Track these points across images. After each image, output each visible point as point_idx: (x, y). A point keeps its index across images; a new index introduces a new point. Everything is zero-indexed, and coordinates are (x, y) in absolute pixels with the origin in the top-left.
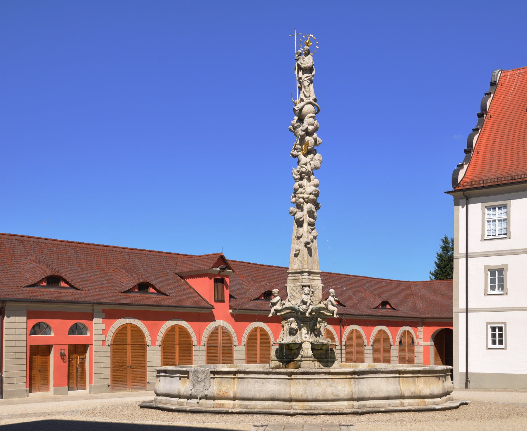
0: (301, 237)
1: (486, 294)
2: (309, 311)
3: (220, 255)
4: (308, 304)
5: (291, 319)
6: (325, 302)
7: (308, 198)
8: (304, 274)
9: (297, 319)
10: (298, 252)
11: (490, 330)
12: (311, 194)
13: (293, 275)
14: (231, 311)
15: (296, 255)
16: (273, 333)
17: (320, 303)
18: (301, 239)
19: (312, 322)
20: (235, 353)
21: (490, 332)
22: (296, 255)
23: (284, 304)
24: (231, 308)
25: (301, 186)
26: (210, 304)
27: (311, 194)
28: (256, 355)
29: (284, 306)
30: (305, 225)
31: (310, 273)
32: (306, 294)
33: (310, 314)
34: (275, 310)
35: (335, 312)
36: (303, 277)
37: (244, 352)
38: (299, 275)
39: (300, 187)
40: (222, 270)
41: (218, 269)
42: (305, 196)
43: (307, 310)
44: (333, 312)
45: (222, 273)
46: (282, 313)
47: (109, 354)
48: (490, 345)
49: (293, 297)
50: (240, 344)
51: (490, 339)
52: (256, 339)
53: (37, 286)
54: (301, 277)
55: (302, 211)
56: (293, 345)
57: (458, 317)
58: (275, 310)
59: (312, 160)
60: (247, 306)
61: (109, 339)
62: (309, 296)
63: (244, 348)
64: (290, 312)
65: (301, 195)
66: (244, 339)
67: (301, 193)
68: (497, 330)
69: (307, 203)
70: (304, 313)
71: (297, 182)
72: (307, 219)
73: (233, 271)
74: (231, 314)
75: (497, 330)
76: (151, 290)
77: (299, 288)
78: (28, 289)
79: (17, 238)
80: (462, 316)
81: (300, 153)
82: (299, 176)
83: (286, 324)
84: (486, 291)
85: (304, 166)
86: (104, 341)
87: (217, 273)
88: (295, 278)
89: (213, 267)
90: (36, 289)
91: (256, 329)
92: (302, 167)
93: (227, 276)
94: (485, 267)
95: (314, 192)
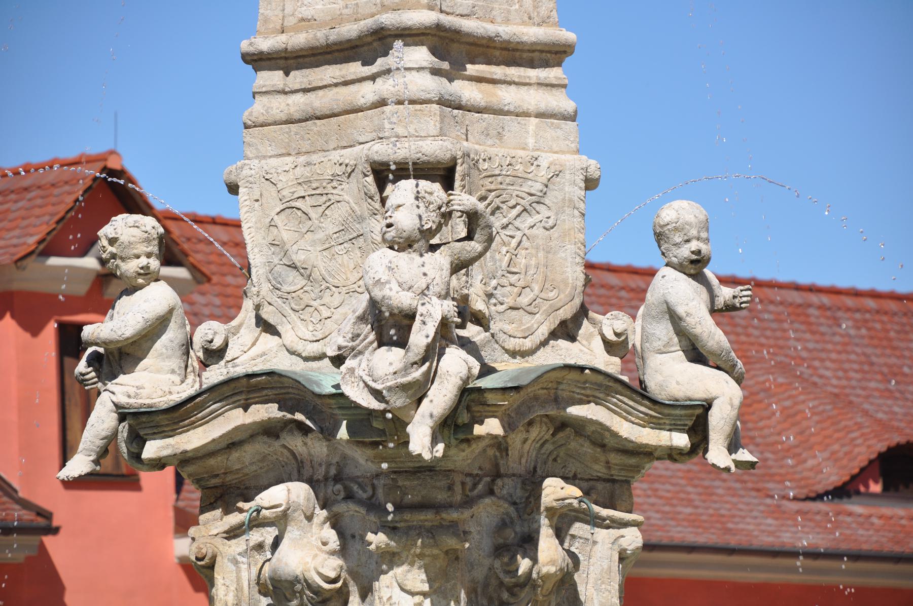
2: (440, 398)
4: (421, 336)
5: (275, 496)
6: (613, 323)
9: (336, 489)
13: (298, 78)
17: (567, 331)
19: (487, 512)
23: (214, 355)
29: (215, 374)
31: (454, 49)
34: (123, 414)
38: (355, 69)
43: (418, 392)
46: (194, 439)
49: (293, 281)
54: (367, 93)
58: (123, 414)
62: (440, 261)
64: (269, 430)
70: (380, 428)
83: (238, 546)
88: (320, 101)
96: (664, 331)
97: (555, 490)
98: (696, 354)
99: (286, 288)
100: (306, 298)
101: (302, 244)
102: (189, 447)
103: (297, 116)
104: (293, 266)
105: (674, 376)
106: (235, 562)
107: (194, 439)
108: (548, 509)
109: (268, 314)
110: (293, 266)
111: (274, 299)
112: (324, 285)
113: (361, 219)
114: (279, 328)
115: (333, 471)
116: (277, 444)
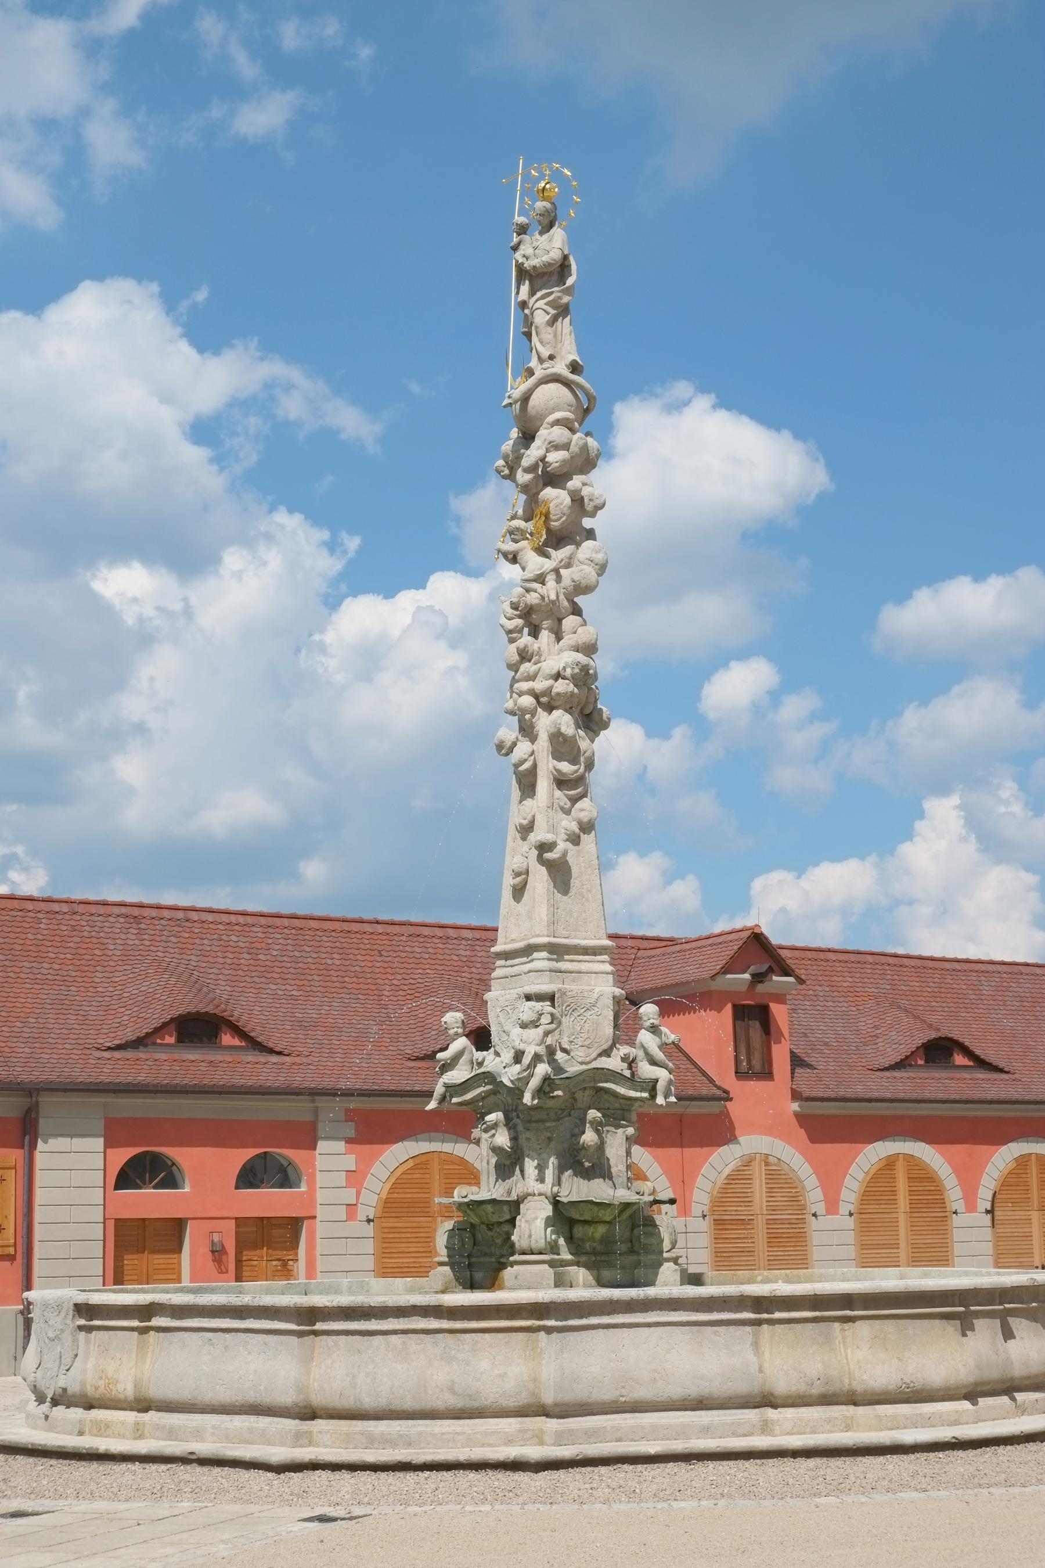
2: (534, 1082)
3: (747, 934)
4: (526, 1060)
5: (491, 1118)
6: (624, 1050)
7: (548, 692)
8: (536, 955)
10: (519, 879)
12: (558, 676)
14: (795, 1106)
15: (518, 892)
16: (817, 1172)
17: (607, 1053)
19: (567, 1122)
20: (815, 1239)
24: (796, 1096)
26: (719, 1088)
27: (558, 676)
28: (896, 1246)
30: (544, 785)
31: (557, 951)
32: (524, 1026)
33: (540, 1092)
35: (661, 1086)
37: (850, 1237)
40: (758, 978)
41: (747, 976)
42: (539, 685)
43: (526, 1081)
44: (652, 1086)
45: (760, 988)
46: (468, 1096)
47: (369, 1246)
50: (832, 1207)
52: (894, 1192)
53: (146, 1045)
55: (533, 739)
56: (489, 1208)
58: (447, 1086)
59: (568, 566)
60: (859, 1090)
61: (370, 1201)
62: (540, 1031)
63: (850, 1222)
66: (850, 1194)
69: (550, 708)
72: (547, 766)
73: (800, 981)
74: (797, 1115)
76: (227, 1039)
78: (117, 1054)
79: (124, 910)
81: (524, 543)
85: (536, 586)
86: (351, 1209)
87: (744, 988)
89: (726, 970)
90: (142, 1055)
91: (890, 1163)
92: (528, 591)
93: (781, 999)
95: (569, 671)
96: (641, 1054)
97: (593, 1114)
98: (653, 1062)
105: (647, 1071)
107: (468, 1096)
108: (590, 1122)
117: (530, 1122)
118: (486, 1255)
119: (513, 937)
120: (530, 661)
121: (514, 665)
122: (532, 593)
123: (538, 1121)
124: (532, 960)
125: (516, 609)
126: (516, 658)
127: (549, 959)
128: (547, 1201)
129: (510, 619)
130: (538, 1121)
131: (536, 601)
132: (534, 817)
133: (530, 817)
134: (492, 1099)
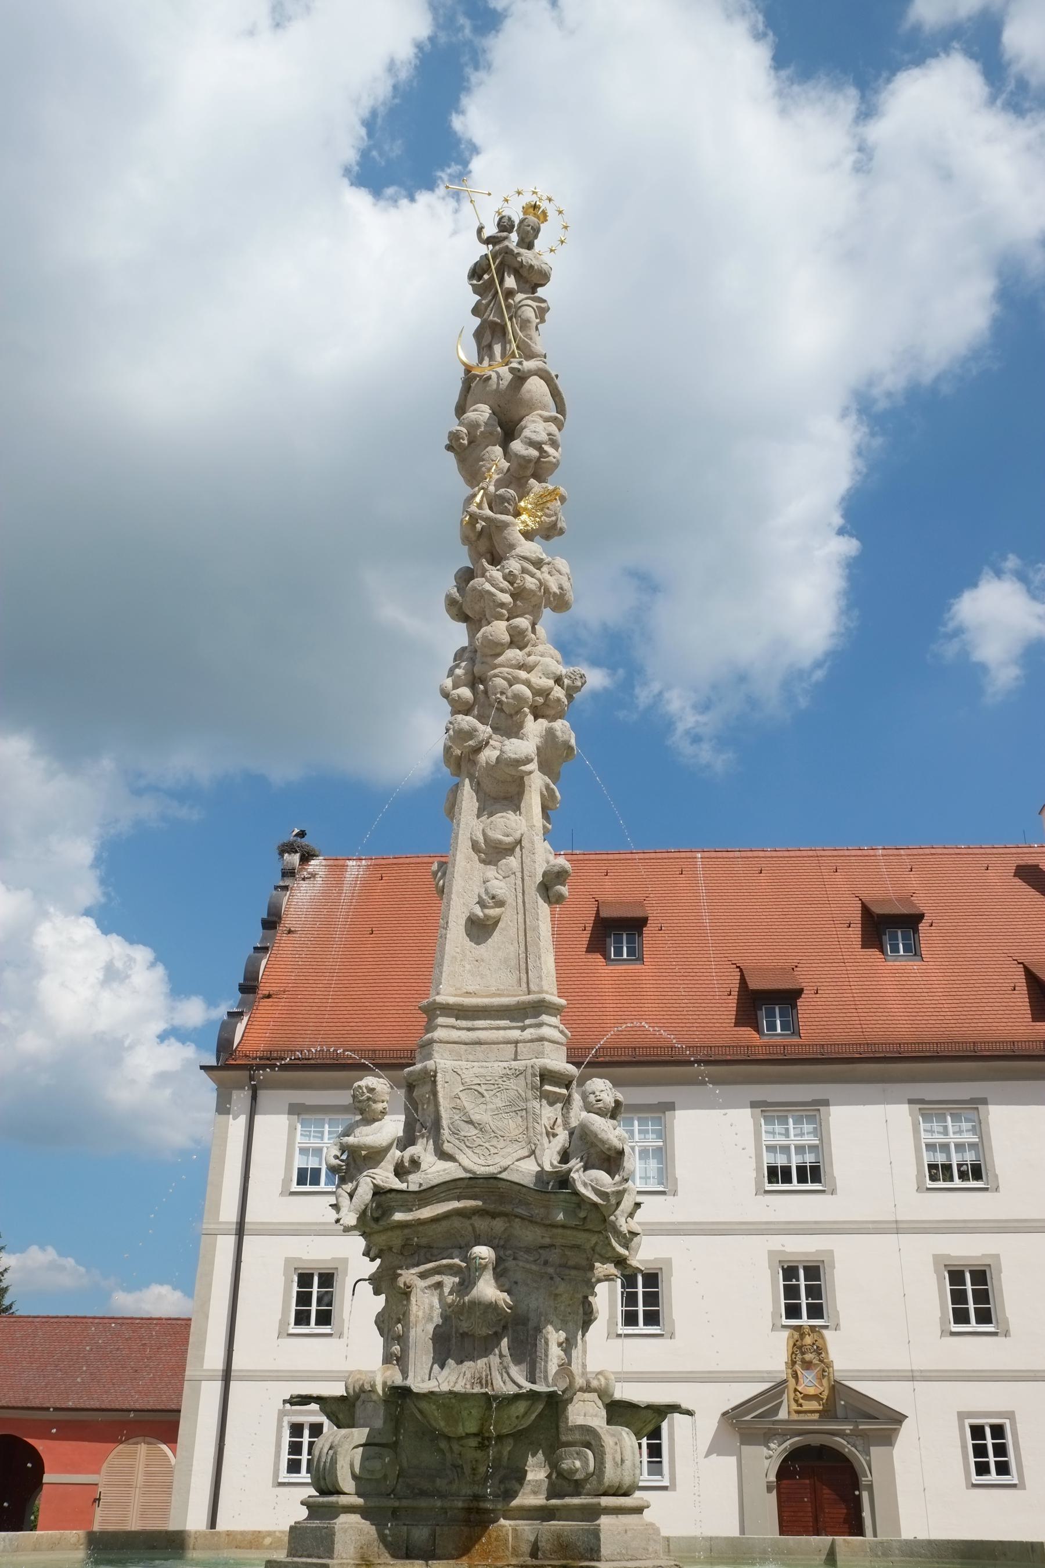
0: (508, 850)
1: (284, 1333)
5: (483, 1252)
7: (545, 693)
8: (545, 1018)
11: (286, 1432)
12: (558, 681)
15: (480, 929)
18: (513, 862)
21: (286, 1439)
22: (480, 929)
25: (517, 640)
36: (545, 1031)
39: (512, 644)
46: (426, 1213)
48: (284, 1476)
51: (285, 1457)
54: (515, 1034)
57: (197, 1392)
65: (523, 674)
67: (522, 667)
68: (306, 1432)
71: (499, 617)
75: (306, 1432)
77: (517, 1086)
80: (211, 1391)
82: (506, 598)
84: (283, 1323)
85: (531, 568)
94: (288, 1261)
99: (463, 1133)
100: (479, 1141)
101: (477, 1110)
102: (422, 1217)
103: (467, 1041)
104: (470, 1122)
106: (422, 1291)
107: (426, 1213)
109: (447, 1147)
110: (470, 1122)
111: (452, 1139)
112: (493, 1135)
113: (527, 1100)
114: (457, 1157)
115: (502, 1243)
116: (467, 1222)
117: (564, 1266)
118: (423, 1493)
119: (470, 989)
120: (521, 649)
121: (502, 645)
122: (527, 577)
123: (576, 1268)
124: (540, 1025)
125: (512, 584)
126: (506, 638)
127: (562, 1032)
128: (600, 1404)
129: (502, 591)
130: (576, 1268)
131: (533, 587)
132: (522, 835)
133: (517, 836)
134: (481, 1224)
